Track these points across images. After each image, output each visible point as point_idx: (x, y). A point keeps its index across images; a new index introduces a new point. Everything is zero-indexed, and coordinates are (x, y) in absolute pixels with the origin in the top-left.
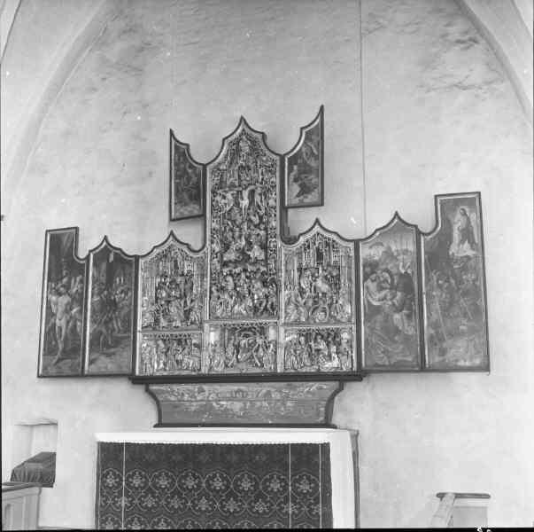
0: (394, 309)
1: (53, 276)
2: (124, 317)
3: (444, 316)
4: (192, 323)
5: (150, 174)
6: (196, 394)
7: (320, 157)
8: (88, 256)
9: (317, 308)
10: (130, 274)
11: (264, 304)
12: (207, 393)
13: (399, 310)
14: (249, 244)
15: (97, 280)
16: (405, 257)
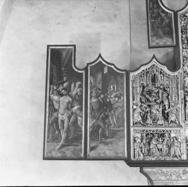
1: (54, 81)
2: (118, 115)
5: (116, 16)
8: (86, 69)
10: (122, 83)
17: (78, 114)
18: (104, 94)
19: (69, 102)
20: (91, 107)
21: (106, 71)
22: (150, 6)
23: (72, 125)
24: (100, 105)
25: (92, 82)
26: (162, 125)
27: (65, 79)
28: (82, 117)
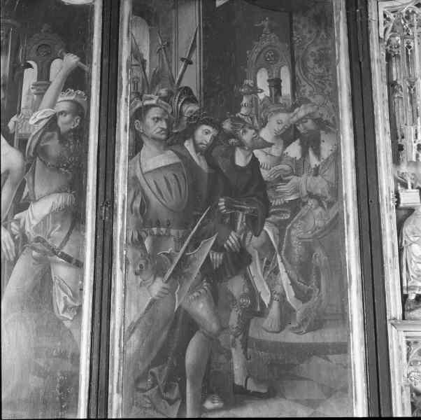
10: (327, 59)
15: (157, 78)
17: (57, 245)
18: (218, 126)
20: (137, 205)
24: (194, 188)
25: (146, 57)
28: (79, 265)
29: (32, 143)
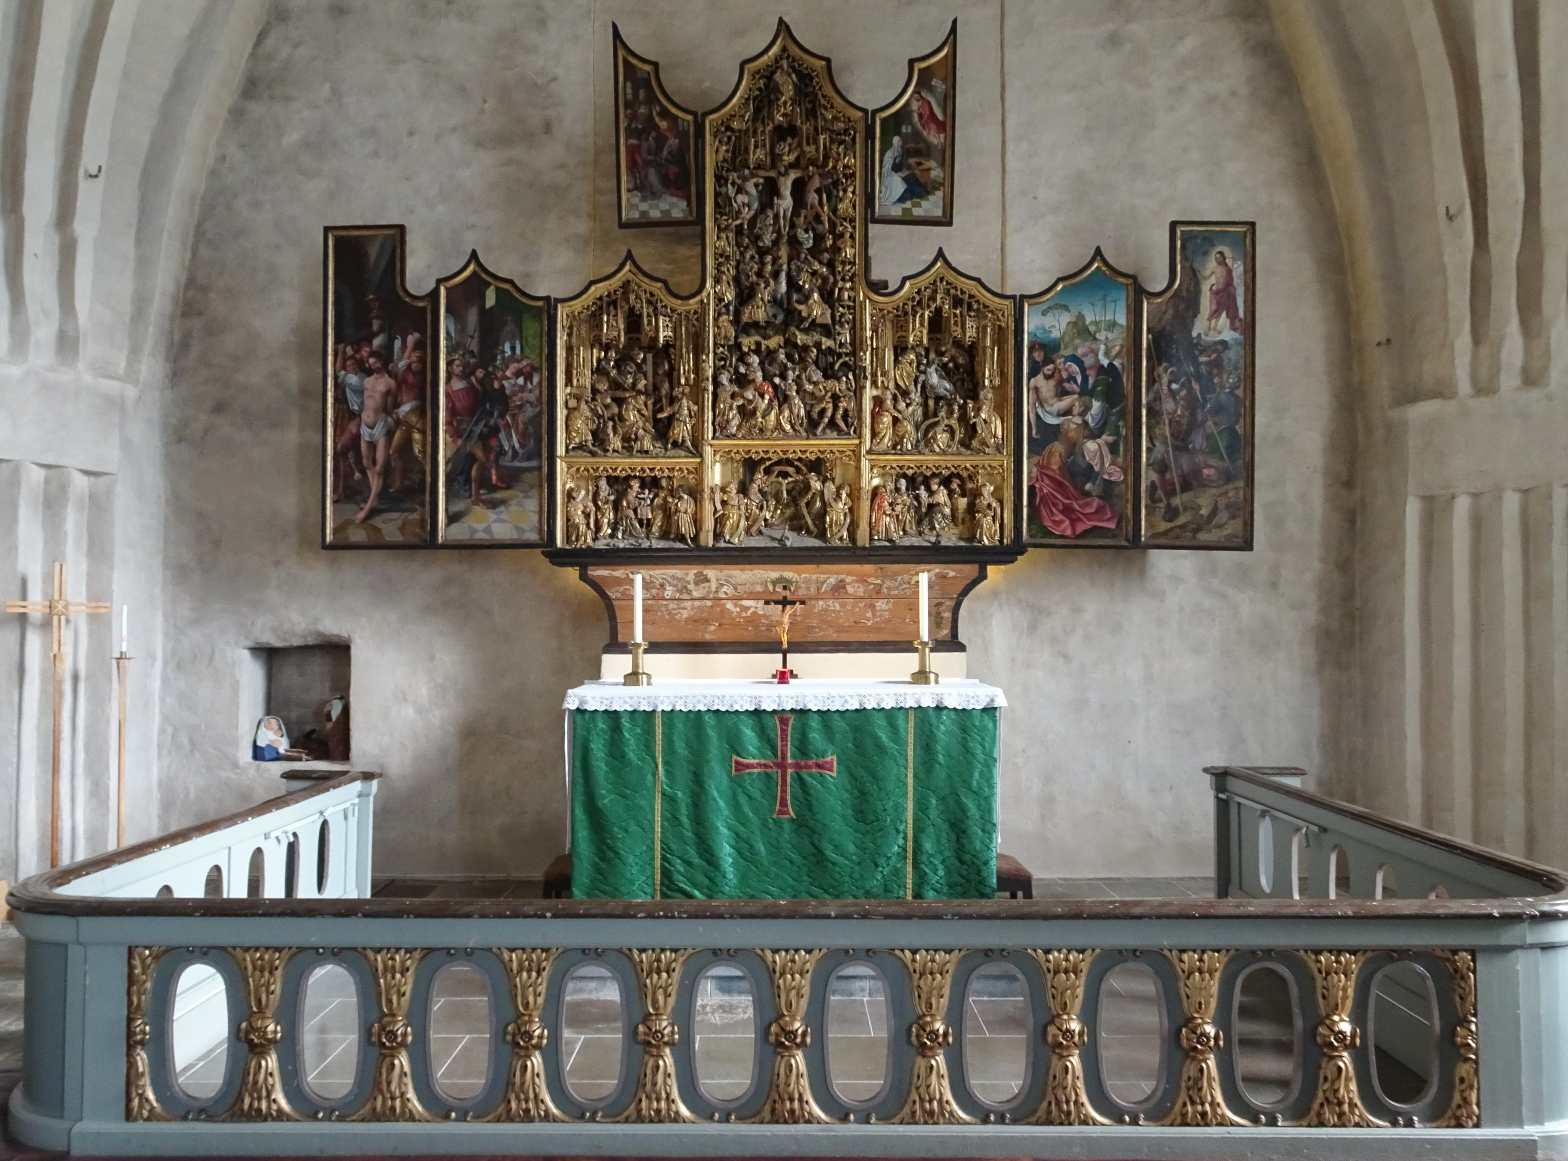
0: (1087, 432)
2: (526, 425)
3: (1176, 448)
4: (675, 444)
6: (691, 587)
7: (947, 126)
9: (936, 424)
11: (829, 413)
12: (714, 585)
13: (1094, 435)
14: (792, 284)
16: (1110, 336)
18: (486, 369)
19: (388, 393)
21: (491, 299)
22: (625, 93)
23: (396, 455)
26: (647, 452)
27: (376, 325)
29: (400, 377)
